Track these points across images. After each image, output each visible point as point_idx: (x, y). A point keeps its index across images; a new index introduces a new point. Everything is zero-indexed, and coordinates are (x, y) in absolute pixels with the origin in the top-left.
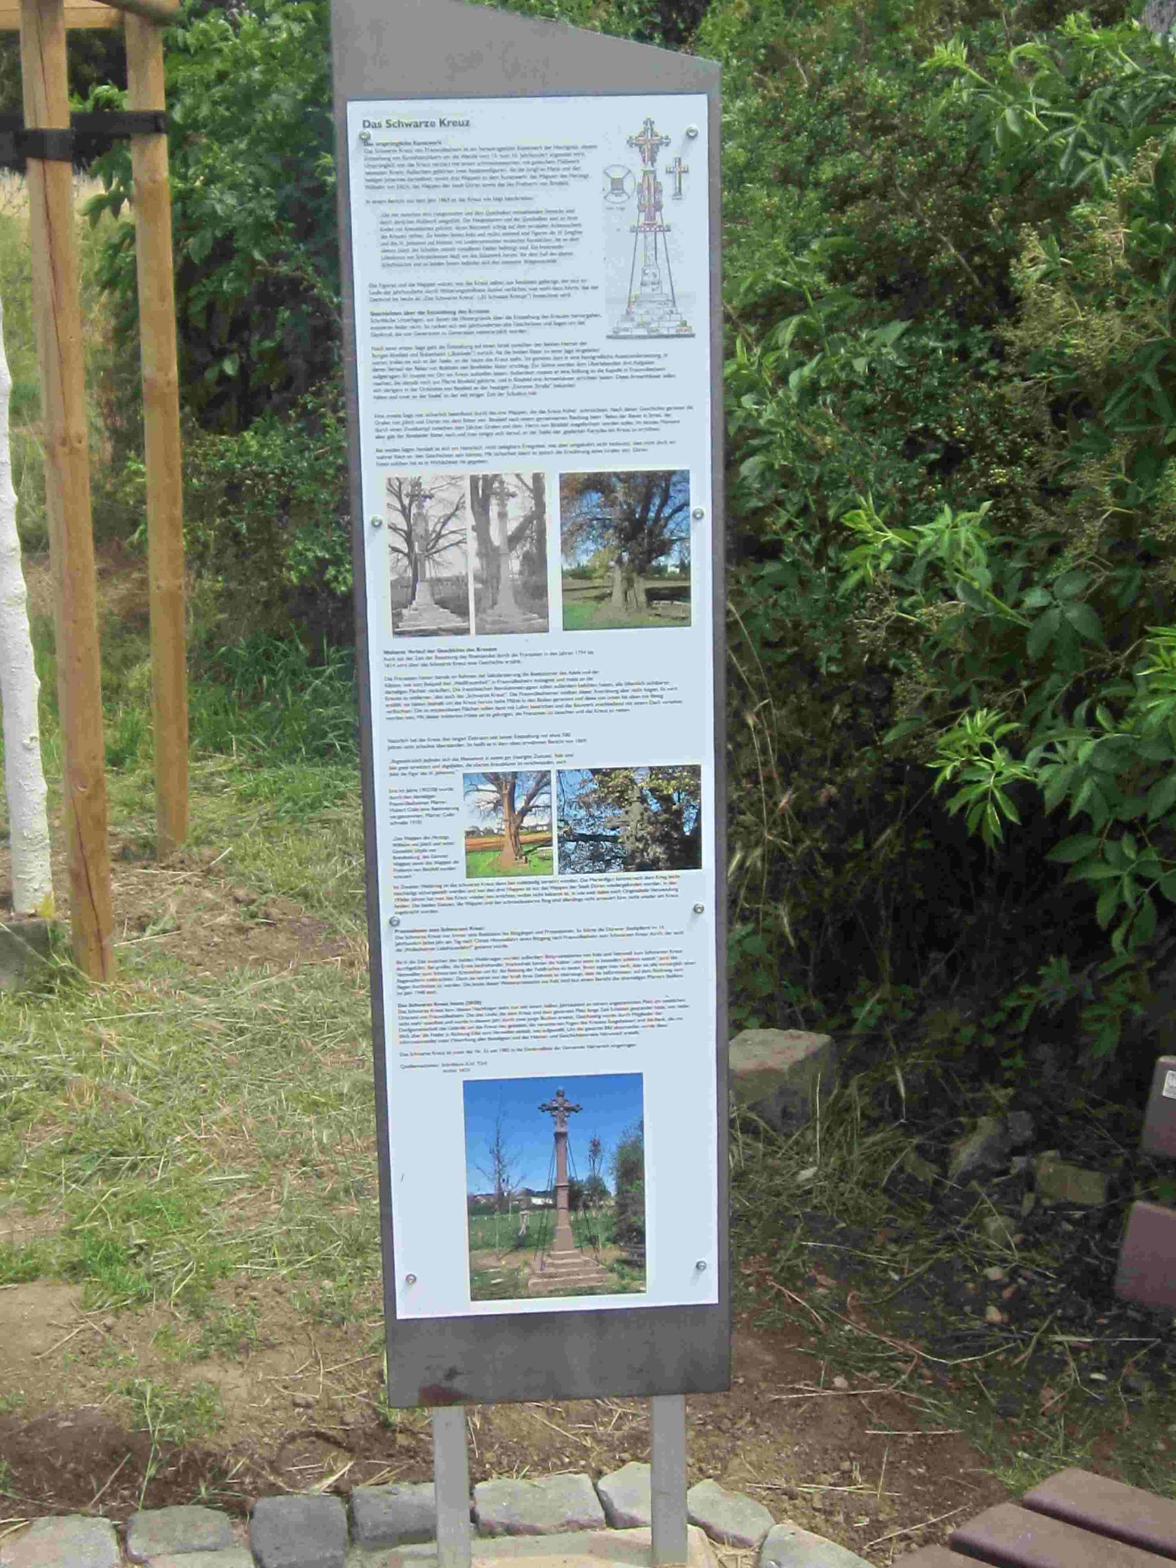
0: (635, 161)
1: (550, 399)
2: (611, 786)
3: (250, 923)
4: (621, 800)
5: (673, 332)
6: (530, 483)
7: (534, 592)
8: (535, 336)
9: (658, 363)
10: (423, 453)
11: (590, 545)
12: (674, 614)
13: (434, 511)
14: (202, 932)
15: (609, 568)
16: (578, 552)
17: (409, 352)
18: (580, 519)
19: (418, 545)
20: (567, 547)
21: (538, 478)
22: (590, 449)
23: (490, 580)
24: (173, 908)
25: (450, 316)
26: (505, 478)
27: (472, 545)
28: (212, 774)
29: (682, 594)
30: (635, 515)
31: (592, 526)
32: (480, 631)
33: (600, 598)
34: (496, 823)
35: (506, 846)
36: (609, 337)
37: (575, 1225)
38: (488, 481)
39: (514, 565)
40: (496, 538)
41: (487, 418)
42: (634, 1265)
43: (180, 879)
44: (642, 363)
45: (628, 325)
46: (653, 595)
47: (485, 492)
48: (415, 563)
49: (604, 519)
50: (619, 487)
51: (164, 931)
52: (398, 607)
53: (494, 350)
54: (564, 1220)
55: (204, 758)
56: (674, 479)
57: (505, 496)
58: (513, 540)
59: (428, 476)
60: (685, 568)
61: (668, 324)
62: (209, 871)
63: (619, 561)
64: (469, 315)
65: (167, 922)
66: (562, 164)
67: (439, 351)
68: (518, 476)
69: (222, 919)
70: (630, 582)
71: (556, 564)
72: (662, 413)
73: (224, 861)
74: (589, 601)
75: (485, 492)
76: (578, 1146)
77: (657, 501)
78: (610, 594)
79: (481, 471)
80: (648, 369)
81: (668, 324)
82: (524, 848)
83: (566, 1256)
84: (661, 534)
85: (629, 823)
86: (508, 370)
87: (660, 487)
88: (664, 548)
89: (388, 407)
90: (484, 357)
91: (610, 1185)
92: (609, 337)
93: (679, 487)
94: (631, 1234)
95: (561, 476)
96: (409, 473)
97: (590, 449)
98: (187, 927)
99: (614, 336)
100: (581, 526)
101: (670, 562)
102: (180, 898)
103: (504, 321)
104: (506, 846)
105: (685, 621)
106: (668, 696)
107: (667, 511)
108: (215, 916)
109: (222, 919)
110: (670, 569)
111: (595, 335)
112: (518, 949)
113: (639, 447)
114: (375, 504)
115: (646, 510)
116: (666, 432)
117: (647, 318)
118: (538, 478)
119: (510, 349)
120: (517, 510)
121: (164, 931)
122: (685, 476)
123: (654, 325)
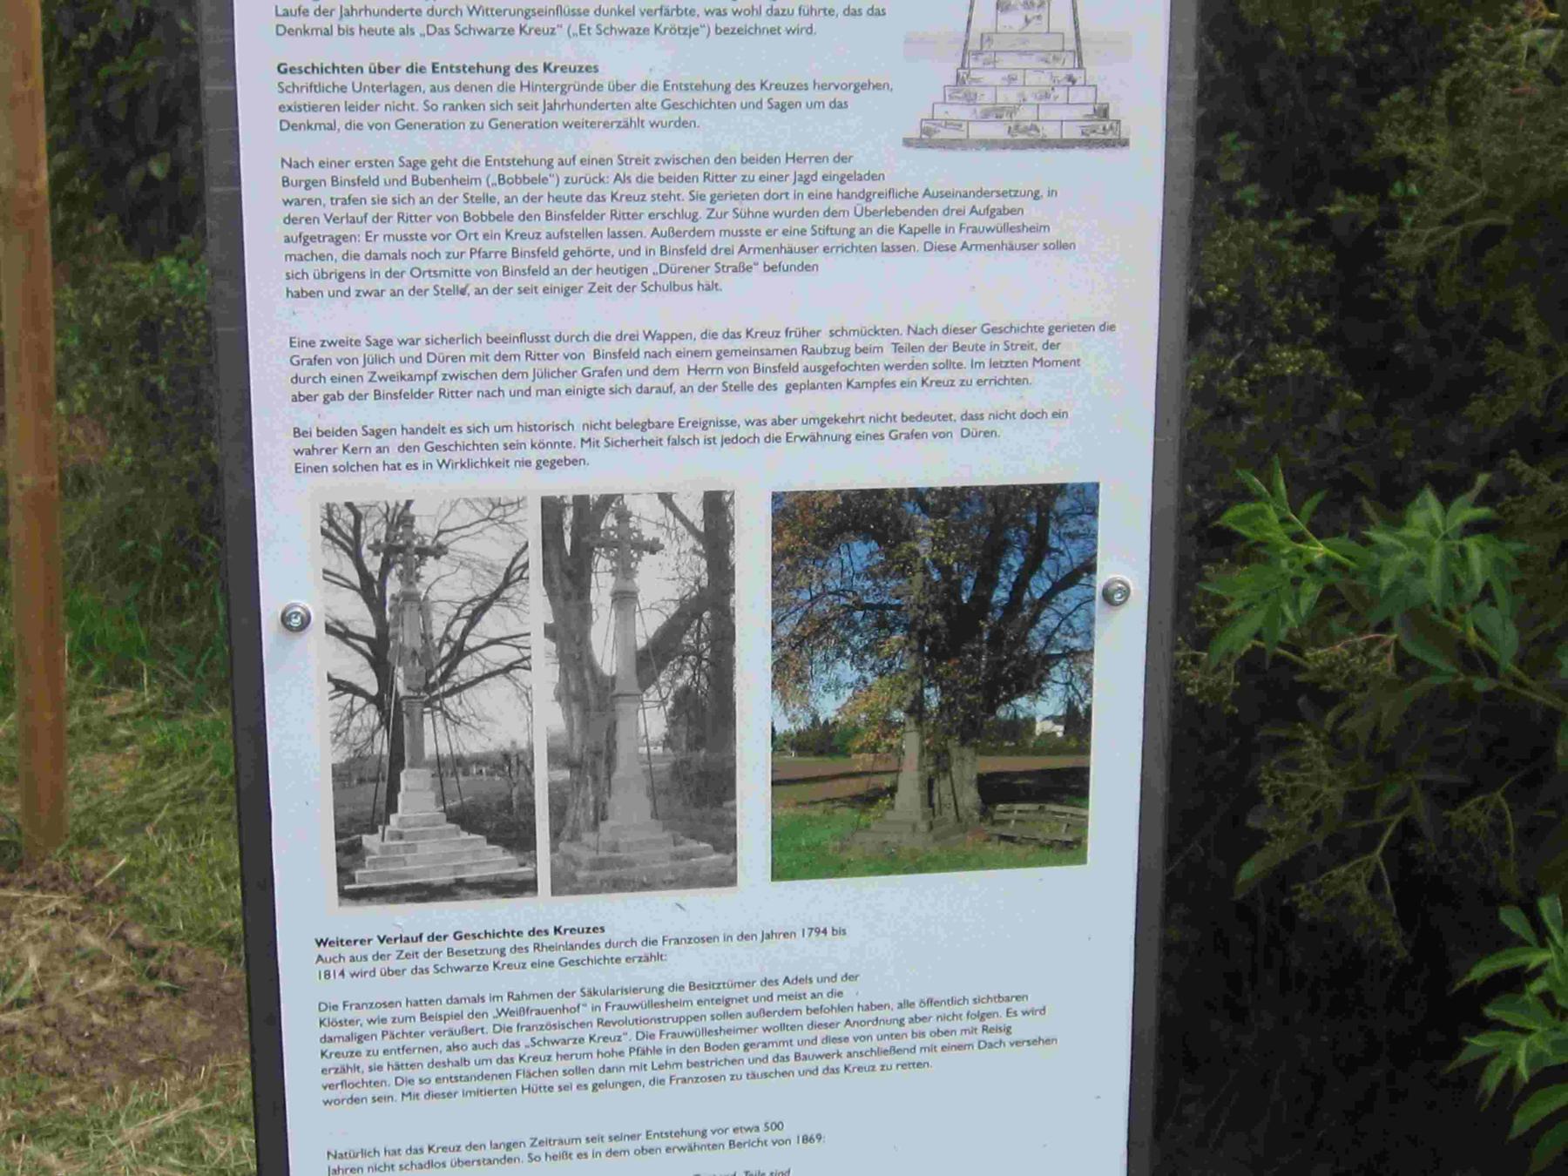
1: (750, 301)
3: (145, 988)
5: (1072, 132)
6: (696, 515)
7: (700, 789)
9: (1033, 213)
10: (420, 440)
11: (846, 671)
12: (1044, 834)
13: (446, 586)
14: (73, 1008)
15: (889, 727)
16: (815, 686)
17: (384, 174)
18: (821, 608)
19: (404, 672)
20: (788, 672)
21: (716, 504)
22: (851, 429)
23: (588, 759)
24: (33, 964)
25: (498, 78)
26: (632, 504)
27: (545, 673)
28: (113, 719)
29: (1071, 785)
30: (947, 592)
31: (852, 626)
32: (564, 884)
33: (868, 800)
36: (908, 142)
38: (589, 510)
39: (649, 721)
40: (606, 654)
41: (588, 348)
43: (51, 907)
44: (992, 213)
45: (960, 112)
46: (995, 790)
47: (578, 540)
49: (883, 607)
50: (923, 524)
51: (20, 1003)
53: (609, 171)
55: (104, 693)
56: (1062, 505)
57: (629, 548)
58: (652, 659)
59: (433, 495)
60: (1077, 722)
61: (1064, 113)
62: (92, 896)
63: (917, 709)
64: (540, 78)
65: (22, 989)
67: (461, 172)
68: (666, 498)
69: (105, 983)
70: (939, 761)
71: (758, 716)
72: (1039, 339)
73: (118, 875)
74: (840, 812)
75: (578, 540)
77: (1015, 561)
78: (892, 790)
79: (565, 484)
80: (1004, 225)
81: (1064, 113)
84: (1022, 640)
86: (645, 226)
87: (1027, 528)
88: (1029, 677)
89: (325, 319)
90: (584, 190)
92: (908, 142)
93: (1072, 526)
95: (776, 498)
96: (379, 489)
97: (851, 429)
98: (51, 998)
99: (925, 139)
100: (824, 623)
101: (1043, 710)
102: (46, 946)
103: (635, 97)
105: (1071, 848)
106: (1023, 1028)
107: (1039, 585)
108: (93, 980)
109: (105, 983)
110: (1041, 727)
111: (871, 138)
113: (974, 426)
114: (293, 568)
115: (987, 580)
116: (1042, 389)
117: (1009, 96)
118: (716, 504)
119: (650, 170)
120: (664, 581)
121: (20, 1003)
122: (1085, 500)
123: (1026, 114)
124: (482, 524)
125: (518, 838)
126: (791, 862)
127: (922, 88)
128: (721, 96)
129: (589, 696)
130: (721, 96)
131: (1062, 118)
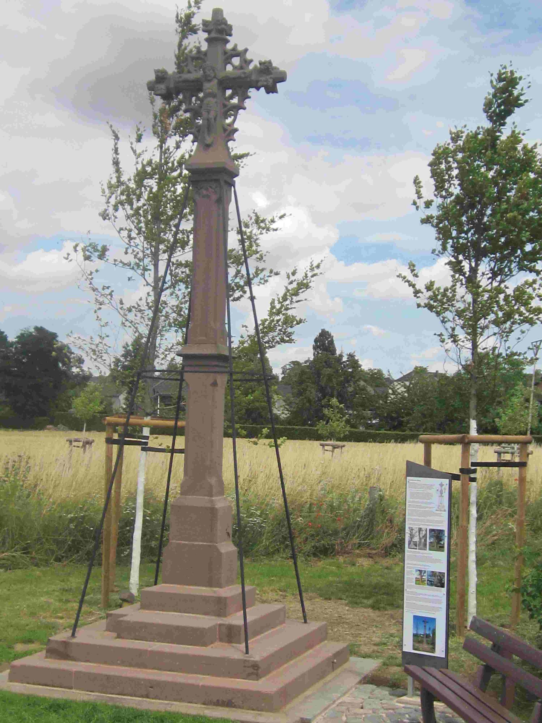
0: (439, 487)
1: (428, 518)
2: (433, 574)
4: (435, 576)
7: (425, 545)
8: (427, 509)
13: (414, 532)
19: (412, 536)
20: (430, 539)
23: (420, 542)
27: (418, 537)
29: (443, 547)
34: (419, 577)
35: (419, 581)
37: (427, 640)
39: (423, 540)
40: (421, 536)
42: (433, 650)
46: (440, 547)
47: (420, 530)
48: (411, 538)
52: (409, 544)
54: (425, 640)
58: (423, 537)
59: (414, 527)
60: (444, 543)
66: (430, 487)
75: (420, 530)
76: (427, 627)
82: (423, 581)
83: (425, 646)
85: (435, 580)
87: (441, 532)
88: (441, 541)
89: (410, 517)
91: (431, 635)
94: (433, 643)
96: (411, 526)
99: (437, 510)
101: (442, 542)
104: (419, 581)
111: (434, 510)
112: (421, 596)
113: (439, 526)
114: (407, 530)
120: (424, 533)
124: (416, 528)
125: (416, 546)
126: (430, 550)
127: (436, 508)
128: (427, 507)
129: (420, 539)
130: (427, 507)
131: (443, 510)
